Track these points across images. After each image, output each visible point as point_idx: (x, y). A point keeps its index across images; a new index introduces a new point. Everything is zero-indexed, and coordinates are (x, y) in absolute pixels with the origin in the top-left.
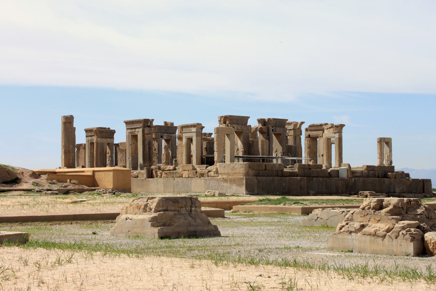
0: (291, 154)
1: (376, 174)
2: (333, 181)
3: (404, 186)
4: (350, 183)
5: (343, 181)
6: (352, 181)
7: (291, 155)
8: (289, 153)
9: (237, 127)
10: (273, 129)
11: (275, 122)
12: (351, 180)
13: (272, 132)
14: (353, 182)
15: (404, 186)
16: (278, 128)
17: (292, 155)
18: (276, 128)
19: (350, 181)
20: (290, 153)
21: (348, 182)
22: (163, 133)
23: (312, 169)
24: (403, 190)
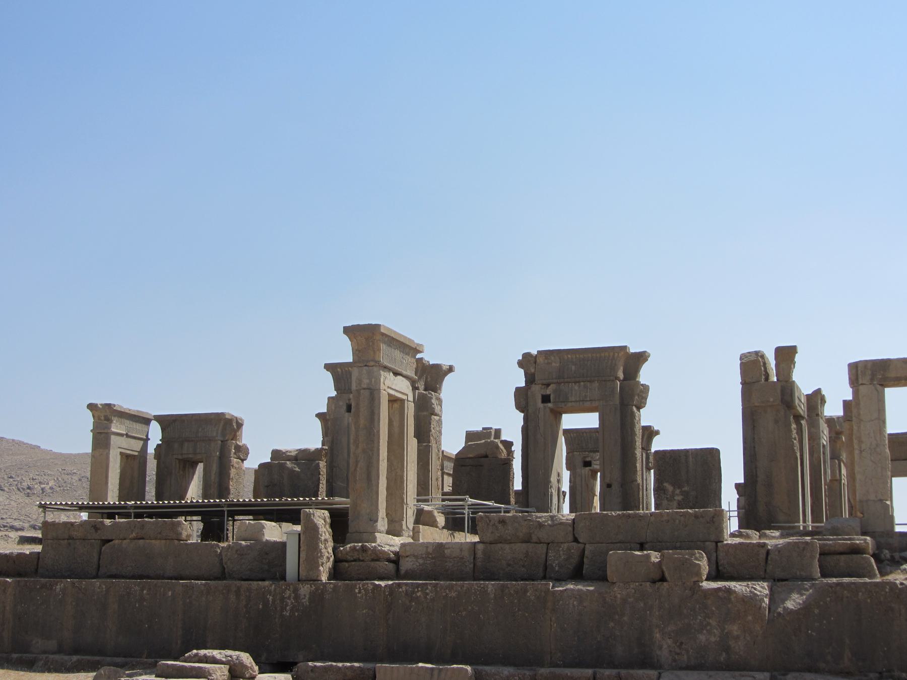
0: (679, 488)
1: (558, 558)
2: (170, 593)
3: (735, 629)
4: (283, 609)
5: (232, 597)
6: (297, 597)
7: (678, 491)
8: (666, 484)
10: (548, 393)
11: (556, 365)
12: (288, 592)
13: (540, 405)
14: (306, 601)
15: (735, 629)
16: (576, 388)
17: (686, 489)
19: (283, 599)
20: (673, 485)
21: (265, 604)
22: (591, 451)
23: (116, 542)
24: (727, 649)
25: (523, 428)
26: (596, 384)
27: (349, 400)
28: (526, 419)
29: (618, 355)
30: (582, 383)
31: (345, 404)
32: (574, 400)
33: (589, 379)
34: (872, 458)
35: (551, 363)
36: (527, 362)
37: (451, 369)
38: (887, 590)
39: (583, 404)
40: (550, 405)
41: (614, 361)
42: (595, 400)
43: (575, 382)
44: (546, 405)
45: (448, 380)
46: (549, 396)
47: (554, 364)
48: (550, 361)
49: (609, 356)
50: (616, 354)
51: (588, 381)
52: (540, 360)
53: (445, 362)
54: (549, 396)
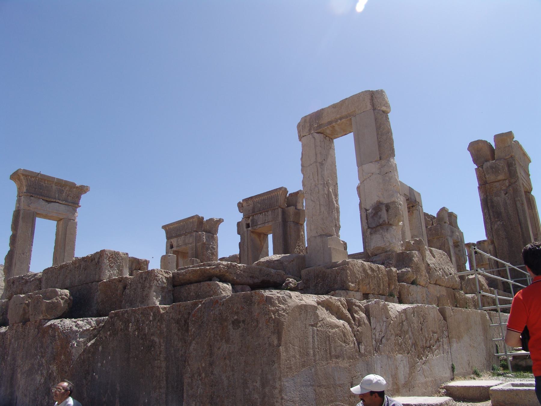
9: (177, 241)
13: (245, 229)
16: (261, 216)
18: (256, 217)
25: (240, 243)
26: (270, 212)
27: (171, 242)
28: (242, 239)
29: (279, 193)
30: (263, 213)
31: (170, 245)
32: (260, 223)
33: (266, 210)
34: (312, 198)
35: (250, 205)
36: (241, 206)
37: (220, 221)
38: (151, 318)
39: (265, 225)
40: (250, 229)
41: (278, 197)
42: (270, 222)
43: (260, 213)
44: (248, 229)
45: (221, 227)
46: (249, 223)
47: (250, 206)
48: (249, 204)
49: (275, 195)
50: (278, 193)
51: (266, 211)
52: (245, 204)
53: (216, 217)
54: (249, 223)
